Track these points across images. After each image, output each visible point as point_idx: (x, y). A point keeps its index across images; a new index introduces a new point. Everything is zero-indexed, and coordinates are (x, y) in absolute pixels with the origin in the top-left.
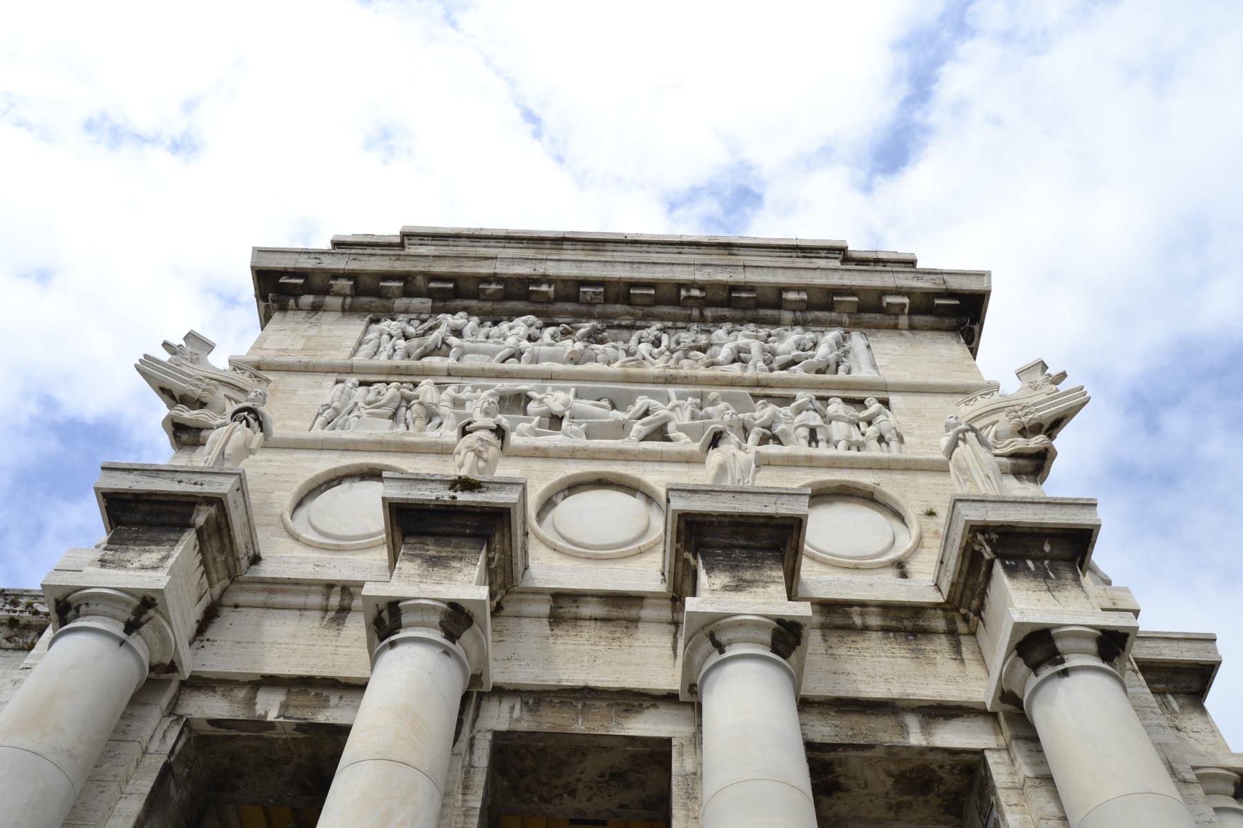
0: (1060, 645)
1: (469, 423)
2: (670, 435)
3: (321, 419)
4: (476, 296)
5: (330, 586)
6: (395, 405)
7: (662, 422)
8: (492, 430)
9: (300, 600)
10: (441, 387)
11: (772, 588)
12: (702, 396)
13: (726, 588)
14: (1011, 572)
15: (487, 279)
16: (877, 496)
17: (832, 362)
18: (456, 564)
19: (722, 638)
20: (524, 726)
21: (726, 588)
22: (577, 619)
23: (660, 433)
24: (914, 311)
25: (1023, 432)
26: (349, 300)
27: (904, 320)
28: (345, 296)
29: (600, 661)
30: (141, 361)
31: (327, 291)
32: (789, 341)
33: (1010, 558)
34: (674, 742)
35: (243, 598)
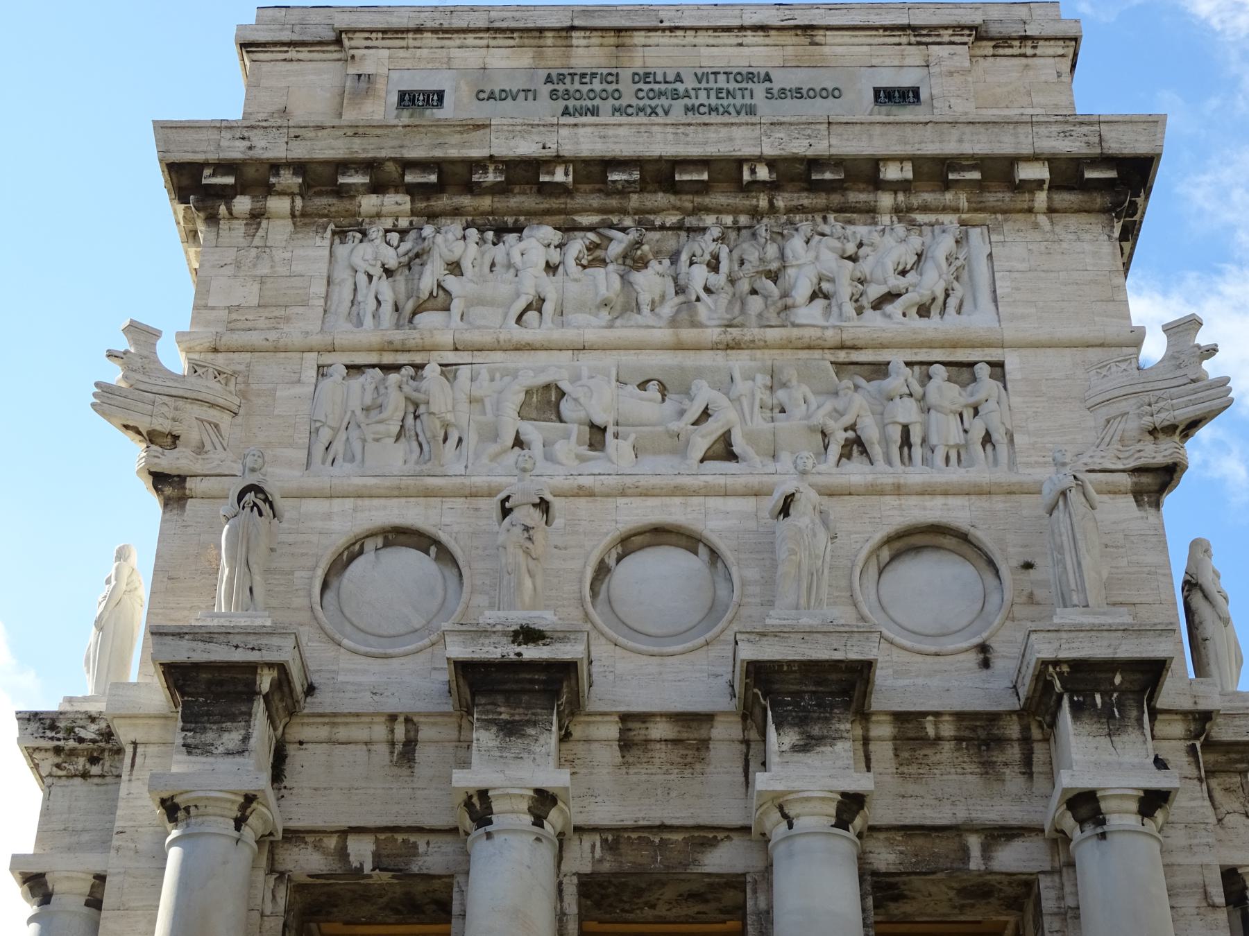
0: (1104, 806)
2: (736, 449)
4: (471, 188)
5: (393, 718)
6: (400, 414)
7: (725, 429)
11: (840, 746)
13: (796, 749)
14: (1078, 710)
16: (970, 537)
18: (531, 731)
19: (791, 810)
21: (796, 749)
22: (647, 741)
23: (725, 451)
24: (1055, 186)
26: (299, 202)
27: (1041, 198)
28: (292, 195)
29: (673, 794)
30: (95, 395)
31: (269, 190)
32: (888, 246)
33: (1078, 693)
34: (749, 879)
35: (307, 733)
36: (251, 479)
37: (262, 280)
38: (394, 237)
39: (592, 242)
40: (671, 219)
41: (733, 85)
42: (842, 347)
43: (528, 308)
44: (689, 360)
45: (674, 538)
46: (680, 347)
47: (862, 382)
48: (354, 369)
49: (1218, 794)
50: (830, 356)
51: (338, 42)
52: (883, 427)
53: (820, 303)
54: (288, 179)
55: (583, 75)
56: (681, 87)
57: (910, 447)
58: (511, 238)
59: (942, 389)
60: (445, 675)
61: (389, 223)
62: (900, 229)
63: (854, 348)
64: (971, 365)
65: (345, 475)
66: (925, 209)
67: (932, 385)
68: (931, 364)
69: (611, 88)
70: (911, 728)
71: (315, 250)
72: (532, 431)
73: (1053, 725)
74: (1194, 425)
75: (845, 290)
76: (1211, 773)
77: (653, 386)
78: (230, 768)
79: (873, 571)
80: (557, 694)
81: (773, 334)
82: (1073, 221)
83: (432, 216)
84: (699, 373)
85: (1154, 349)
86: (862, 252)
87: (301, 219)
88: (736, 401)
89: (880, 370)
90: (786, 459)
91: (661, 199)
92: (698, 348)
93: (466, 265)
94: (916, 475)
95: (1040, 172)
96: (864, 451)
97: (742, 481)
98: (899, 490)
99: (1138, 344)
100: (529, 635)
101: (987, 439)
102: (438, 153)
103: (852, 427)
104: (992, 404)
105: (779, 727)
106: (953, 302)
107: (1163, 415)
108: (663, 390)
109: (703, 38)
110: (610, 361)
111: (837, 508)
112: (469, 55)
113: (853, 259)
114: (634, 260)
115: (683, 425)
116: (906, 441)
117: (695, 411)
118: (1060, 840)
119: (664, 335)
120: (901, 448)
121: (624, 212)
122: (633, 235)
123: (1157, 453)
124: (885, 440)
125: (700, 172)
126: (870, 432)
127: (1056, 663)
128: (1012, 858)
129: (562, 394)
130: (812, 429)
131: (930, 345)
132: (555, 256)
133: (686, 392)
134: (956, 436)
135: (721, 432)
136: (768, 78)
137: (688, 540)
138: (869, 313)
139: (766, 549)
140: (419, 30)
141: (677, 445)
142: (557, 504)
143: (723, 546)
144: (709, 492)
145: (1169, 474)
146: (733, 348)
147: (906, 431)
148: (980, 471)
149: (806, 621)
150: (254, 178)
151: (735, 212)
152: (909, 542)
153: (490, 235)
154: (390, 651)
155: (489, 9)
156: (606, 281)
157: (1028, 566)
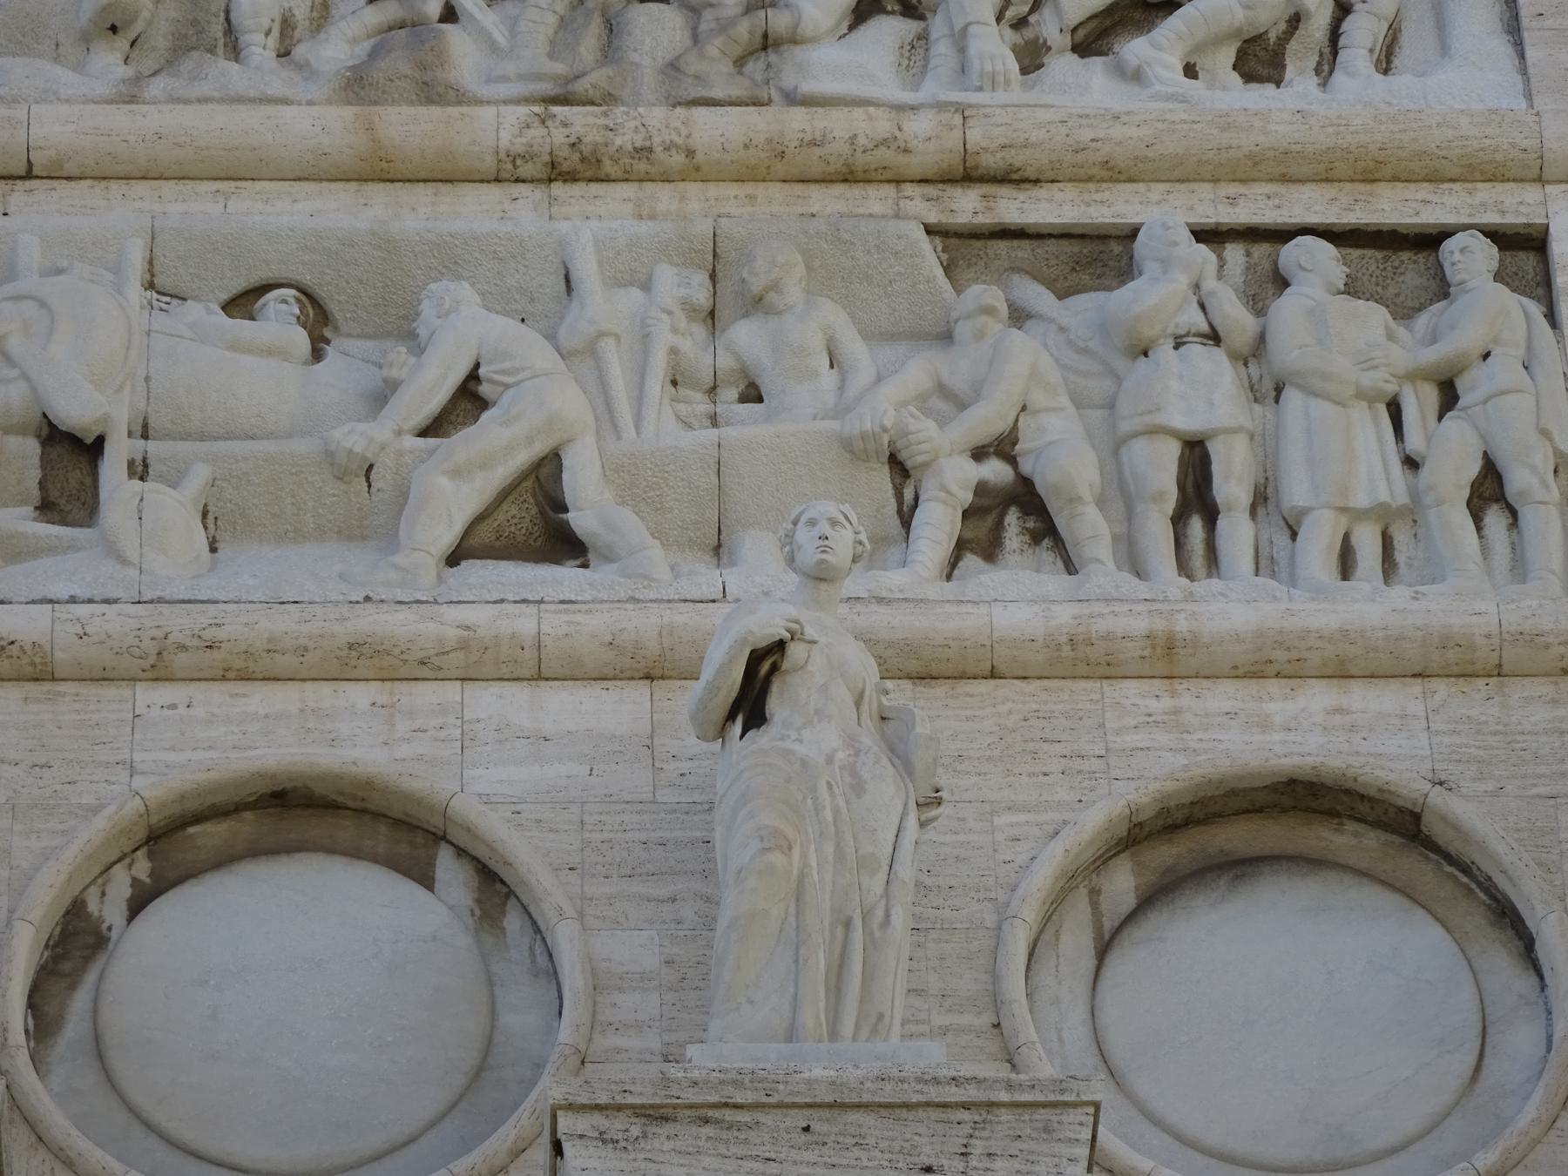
2: (580, 520)
7: (540, 448)
16: (1431, 826)
42: (968, 175)
44: (416, 214)
45: (345, 829)
46: (379, 170)
47: (1037, 296)
50: (921, 205)
52: (1115, 447)
57: (1211, 516)
59: (1328, 319)
63: (1009, 178)
64: (1429, 241)
67: (1287, 308)
77: (280, 311)
79: (1076, 939)
81: (715, 129)
84: (449, 258)
88: (583, 355)
89: (1104, 255)
90: (759, 553)
92: (445, 175)
94: (1232, 607)
96: (1045, 530)
97: (595, 625)
98: (1169, 659)
101: (1489, 489)
103: (1003, 447)
104: (1505, 369)
108: (319, 321)
110: (121, 214)
111: (934, 714)
115: (387, 435)
116: (1197, 494)
117: (431, 387)
119: (317, 124)
120: (1179, 520)
124: (1122, 495)
126: (1065, 458)
130: (854, 450)
131: (1283, 169)
133: (404, 329)
134: (1373, 474)
135: (523, 458)
137: (398, 832)
138: (1063, 66)
139: (681, 862)
141: (362, 502)
143: (527, 855)
144: (476, 664)
146: (571, 177)
147: (1196, 460)
148: (1463, 593)
149: (819, 1071)
152: (1207, 839)
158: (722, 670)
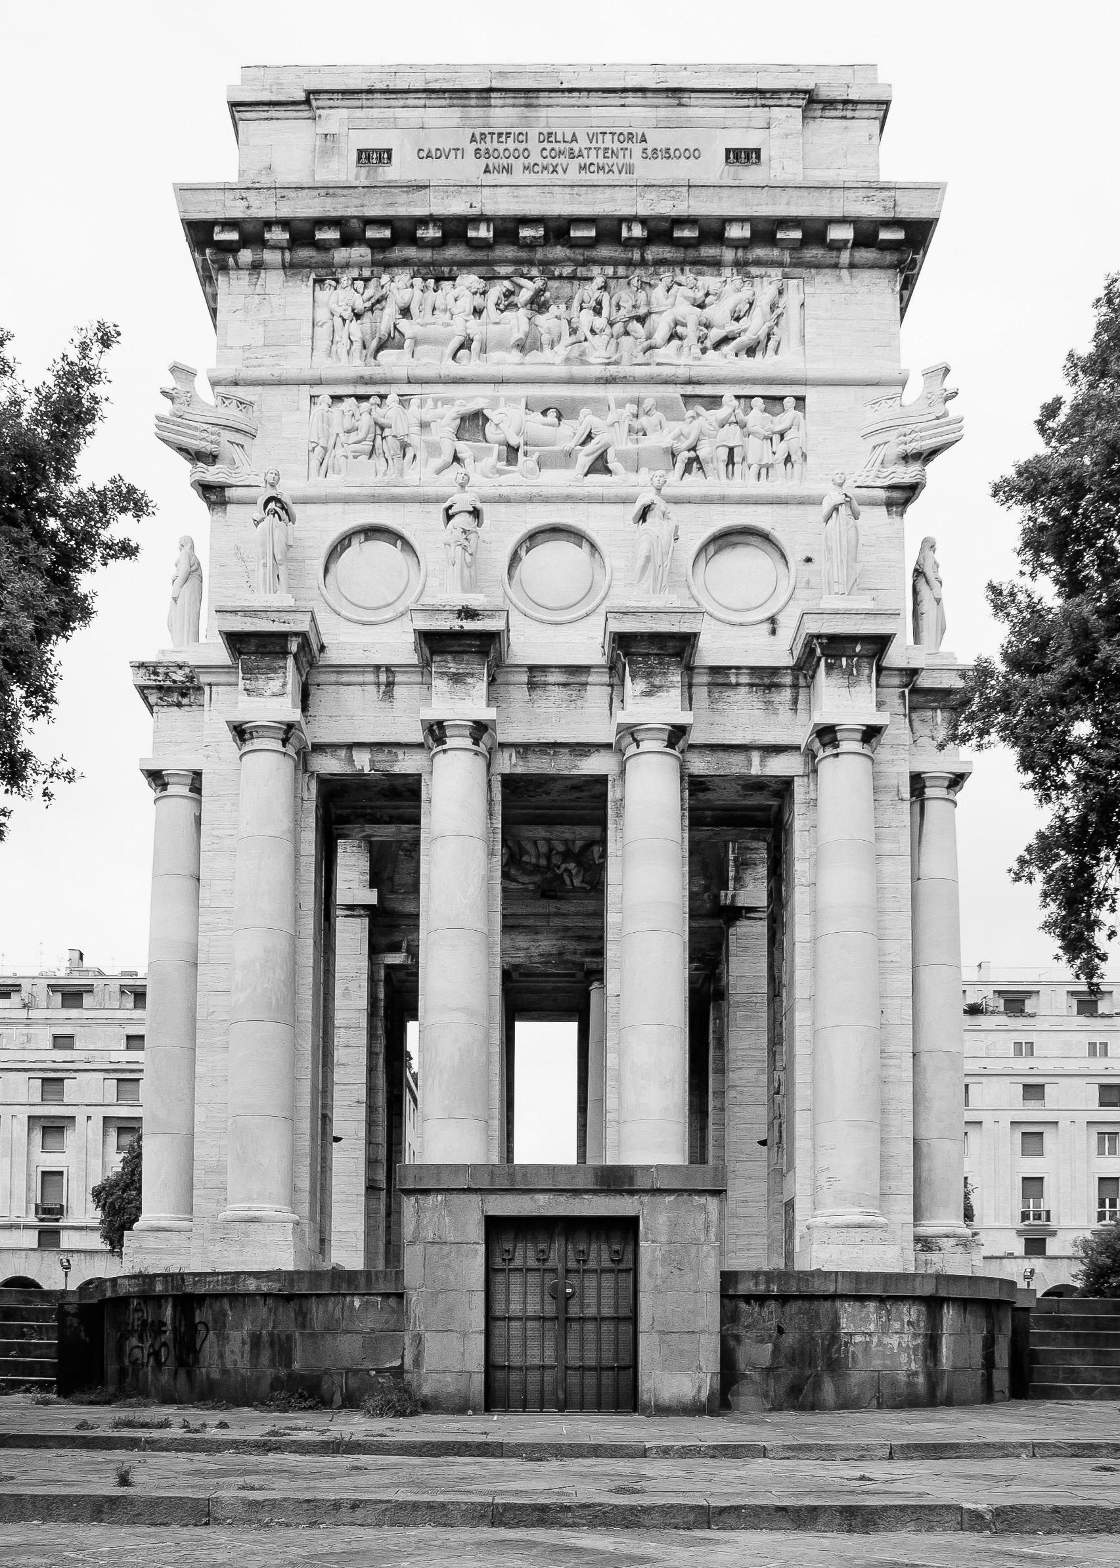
1: (451, 507)
2: (610, 465)
3: (315, 463)
4: (414, 241)
5: (377, 668)
6: (371, 436)
8: (469, 513)
9: (359, 678)
10: (404, 400)
12: (638, 402)
15: (424, 221)
17: (763, 338)
20: (519, 770)
22: (546, 684)
25: (906, 458)
26: (287, 255)
27: (845, 257)
28: (282, 249)
29: (563, 721)
31: (264, 244)
34: (610, 778)
35: (322, 678)
36: (273, 493)
37: (265, 323)
38: (359, 284)
39: (508, 290)
40: (567, 271)
41: (616, 146)
42: (690, 382)
43: (461, 347)
46: (571, 381)
47: (701, 410)
48: (337, 398)
49: (916, 724)
51: (307, 102)
53: (675, 343)
54: (278, 235)
55: (500, 135)
56: (575, 147)
57: (733, 464)
58: (446, 285)
60: (412, 638)
61: (355, 273)
62: (737, 279)
63: (698, 383)
64: (782, 398)
65: (334, 484)
66: (758, 263)
68: (752, 397)
69: (521, 147)
70: (720, 676)
71: (301, 290)
72: (464, 448)
73: (813, 677)
74: (934, 452)
75: (691, 332)
76: (912, 709)
77: (552, 414)
78: (273, 701)
80: (486, 654)
82: (867, 275)
83: (387, 265)
85: (914, 391)
86: (708, 300)
87: (291, 268)
91: (559, 252)
92: (585, 381)
93: (414, 309)
95: (845, 233)
98: (723, 500)
99: (903, 384)
100: (468, 613)
101: (788, 459)
102: (390, 212)
105: (633, 678)
106: (772, 344)
107: (913, 445)
108: (560, 417)
109: (594, 99)
112: (409, 114)
113: (702, 306)
114: (538, 304)
118: (811, 755)
120: (727, 466)
121: (530, 263)
122: (539, 283)
123: (906, 474)
125: (589, 229)
127: (819, 636)
128: (779, 766)
129: (486, 419)
132: (478, 301)
136: (644, 140)
138: (711, 353)
140: (370, 91)
142: (486, 509)
145: (912, 490)
146: (610, 383)
148: (780, 484)
150: (252, 234)
151: (615, 263)
153: (431, 282)
154: (373, 619)
155: (424, 68)
156: (517, 322)
157: (809, 560)
158: (636, 508)
